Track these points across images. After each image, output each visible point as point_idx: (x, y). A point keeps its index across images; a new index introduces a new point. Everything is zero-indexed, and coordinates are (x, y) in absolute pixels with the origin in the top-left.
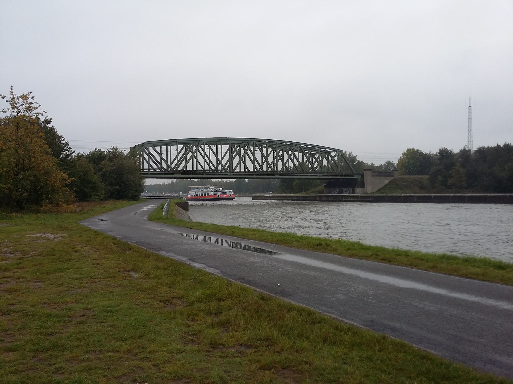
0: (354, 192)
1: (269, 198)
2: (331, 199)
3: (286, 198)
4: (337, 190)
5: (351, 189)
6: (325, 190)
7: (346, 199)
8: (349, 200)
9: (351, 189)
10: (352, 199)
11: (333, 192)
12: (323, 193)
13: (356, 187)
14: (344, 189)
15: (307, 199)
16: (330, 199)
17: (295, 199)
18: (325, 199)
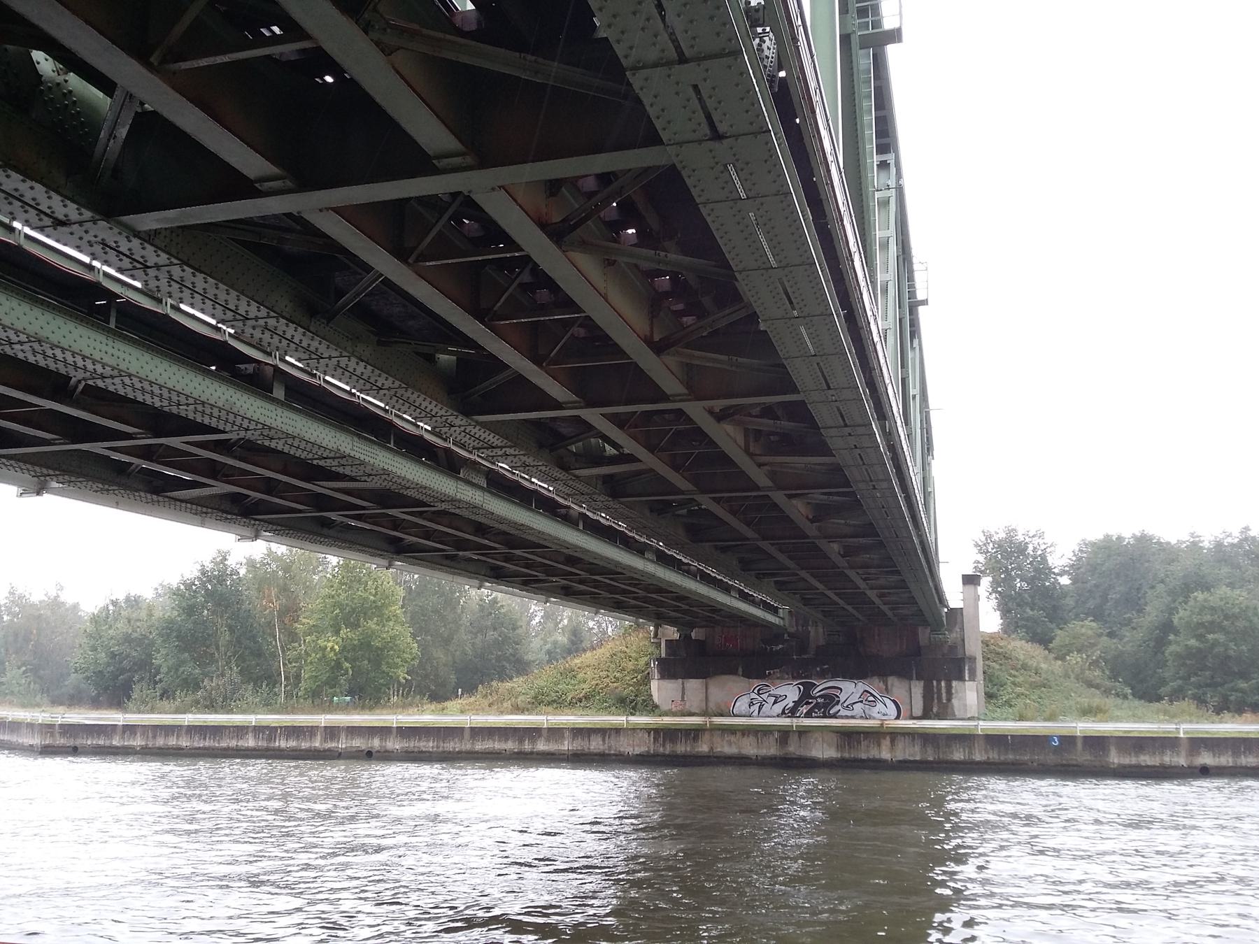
0: (935, 705)
1: (250, 742)
2: (978, 757)
3: (452, 745)
4: (779, 691)
5: (918, 689)
6: (659, 690)
7: (1146, 760)
8: (1182, 761)
9: (918, 689)
10: (1206, 759)
11: (742, 705)
12: (652, 708)
13: (961, 678)
14: (850, 690)
15: (704, 748)
16: (958, 755)
17: (566, 746)
18: (913, 752)
